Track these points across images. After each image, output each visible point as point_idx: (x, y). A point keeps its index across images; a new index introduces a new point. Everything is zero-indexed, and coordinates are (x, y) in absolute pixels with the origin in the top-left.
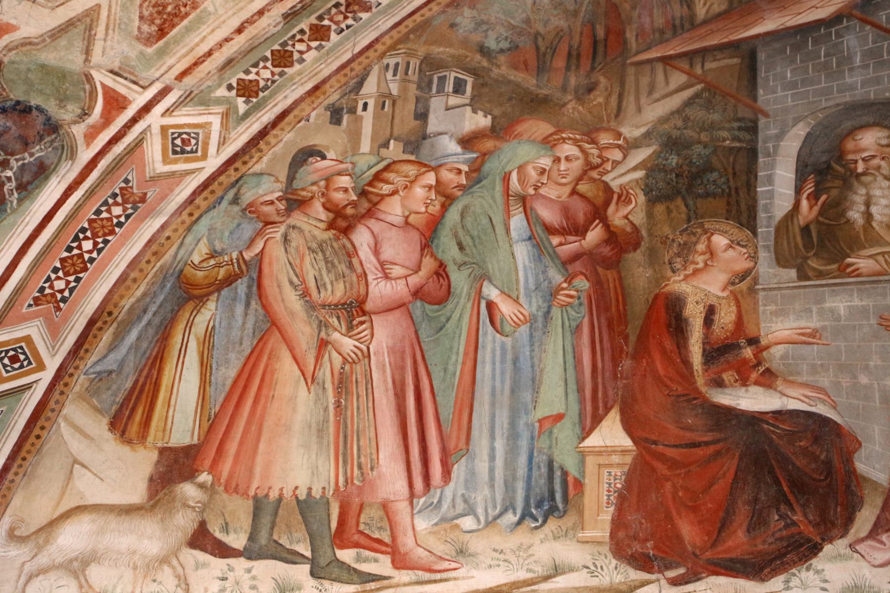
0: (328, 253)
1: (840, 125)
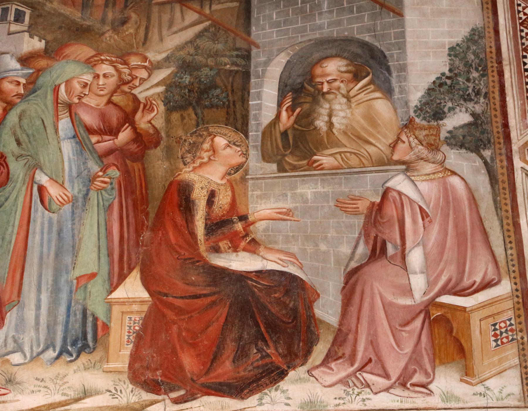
1: (312, 55)
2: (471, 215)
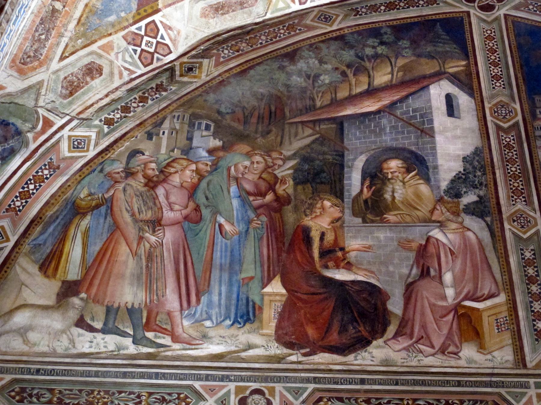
0: (144, 198)
2: (480, 255)
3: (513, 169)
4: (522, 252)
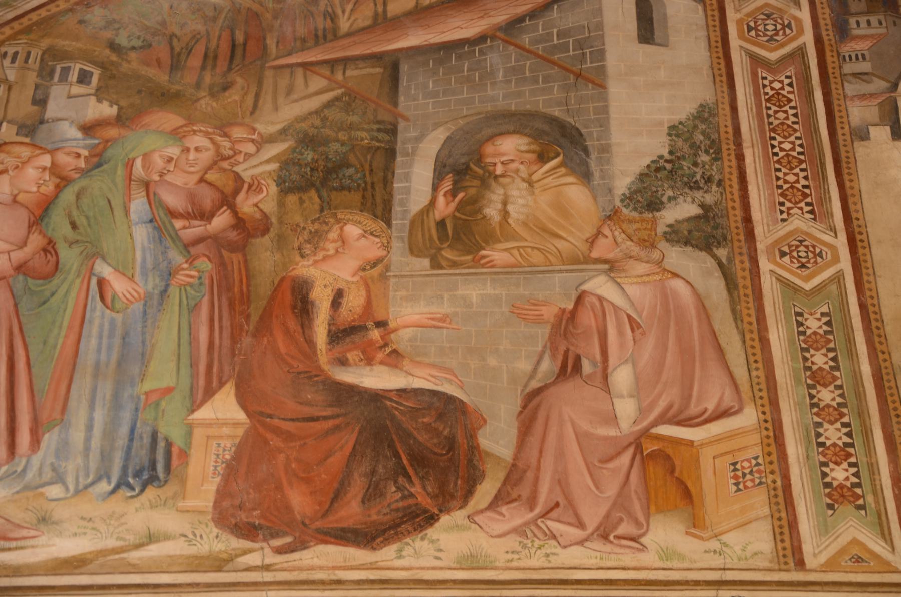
3: (787, 146)
4: (800, 319)
